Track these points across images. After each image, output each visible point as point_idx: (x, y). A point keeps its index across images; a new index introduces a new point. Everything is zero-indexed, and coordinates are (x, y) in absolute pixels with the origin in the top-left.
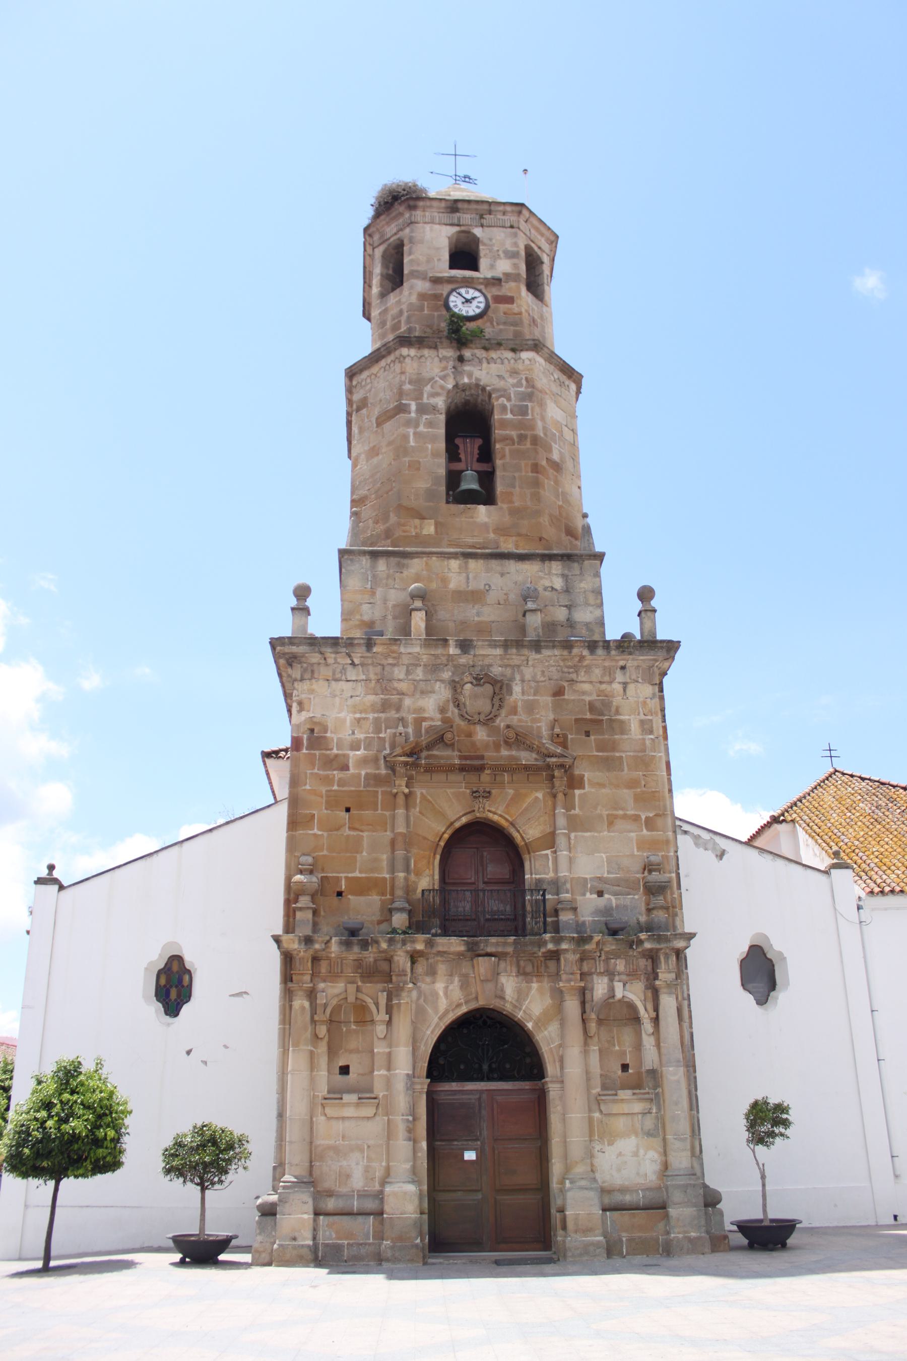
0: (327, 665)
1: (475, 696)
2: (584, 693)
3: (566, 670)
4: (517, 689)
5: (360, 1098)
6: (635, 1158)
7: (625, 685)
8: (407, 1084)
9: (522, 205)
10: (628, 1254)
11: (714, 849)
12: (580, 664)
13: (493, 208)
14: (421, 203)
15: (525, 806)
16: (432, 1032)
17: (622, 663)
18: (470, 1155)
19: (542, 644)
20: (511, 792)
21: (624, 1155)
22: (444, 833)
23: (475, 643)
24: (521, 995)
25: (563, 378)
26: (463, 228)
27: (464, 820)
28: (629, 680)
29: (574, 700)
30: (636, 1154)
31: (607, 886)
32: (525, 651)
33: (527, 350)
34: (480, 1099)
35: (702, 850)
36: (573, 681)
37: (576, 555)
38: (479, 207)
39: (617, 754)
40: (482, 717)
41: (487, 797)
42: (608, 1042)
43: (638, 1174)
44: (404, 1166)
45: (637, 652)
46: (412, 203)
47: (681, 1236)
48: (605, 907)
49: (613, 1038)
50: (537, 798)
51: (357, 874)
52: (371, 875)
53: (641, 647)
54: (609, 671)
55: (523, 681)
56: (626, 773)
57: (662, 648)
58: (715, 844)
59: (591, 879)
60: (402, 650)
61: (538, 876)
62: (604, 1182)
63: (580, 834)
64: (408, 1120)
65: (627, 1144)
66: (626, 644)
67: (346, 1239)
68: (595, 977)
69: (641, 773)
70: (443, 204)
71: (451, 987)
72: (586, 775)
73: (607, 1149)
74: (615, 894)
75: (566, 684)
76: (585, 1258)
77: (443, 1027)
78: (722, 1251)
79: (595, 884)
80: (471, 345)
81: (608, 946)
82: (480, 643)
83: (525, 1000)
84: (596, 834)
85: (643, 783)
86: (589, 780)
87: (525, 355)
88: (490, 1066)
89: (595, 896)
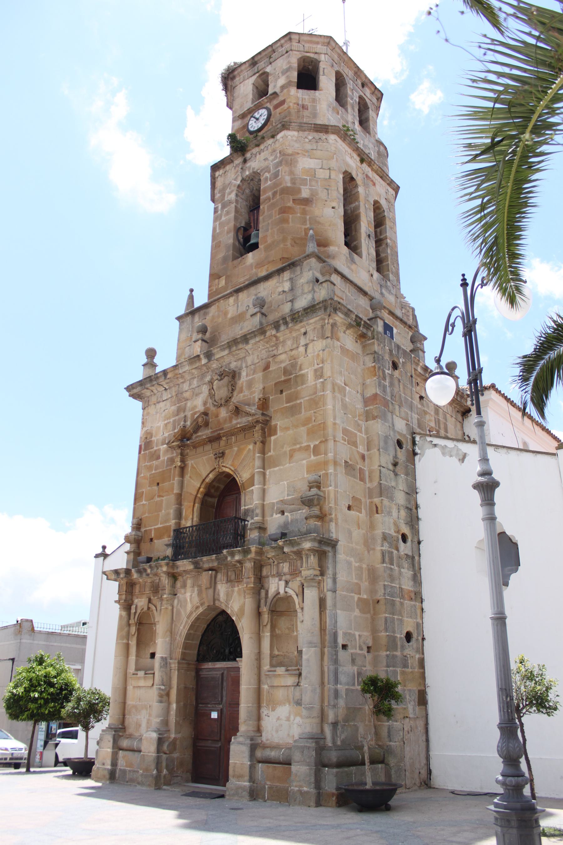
0: (155, 394)
1: (219, 388)
2: (281, 362)
3: (271, 349)
4: (244, 374)
5: (146, 674)
6: (287, 722)
7: (306, 345)
8: (161, 663)
9: (290, 33)
10: (268, 799)
11: (457, 455)
12: (278, 342)
13: (274, 48)
14: (236, 73)
15: (243, 457)
16: (184, 627)
17: (303, 330)
18: (214, 715)
19: (248, 337)
20: (236, 449)
21: (281, 719)
22: (200, 488)
23: (213, 352)
24: (229, 596)
25: (317, 135)
26: (260, 72)
27: (211, 476)
28: (308, 342)
29: (275, 370)
30: (288, 719)
31: (286, 506)
32: (241, 346)
33: (281, 132)
34: (223, 674)
35: (448, 457)
36: (275, 355)
37: (297, 261)
38: (266, 52)
39: (298, 402)
40: (223, 401)
41: (221, 457)
42: (289, 629)
43: (288, 735)
44: (155, 720)
45: (305, 319)
46: (231, 76)
47: (297, 789)
48: (284, 522)
49: (293, 625)
50: (249, 449)
51: (159, 526)
52: (165, 525)
53: (307, 313)
54: (296, 339)
55: (247, 367)
56: (304, 414)
57: (320, 308)
58: (458, 450)
59: (277, 503)
60: (181, 371)
61: (246, 507)
62: (267, 740)
63: (272, 469)
64: (160, 688)
65: (283, 711)
66: (296, 316)
67: (129, 767)
68: (270, 578)
69: (312, 412)
70: (247, 65)
71: (193, 595)
72: (279, 423)
73: (271, 714)
74: (291, 511)
75: (271, 360)
76: (236, 798)
77: (190, 622)
78: (330, 807)
79: (279, 506)
80: (249, 149)
81: (270, 553)
82: (215, 351)
83: (230, 601)
84: (282, 467)
85: (313, 419)
86: (280, 427)
87: (279, 136)
88: (230, 650)
89: (280, 515)
